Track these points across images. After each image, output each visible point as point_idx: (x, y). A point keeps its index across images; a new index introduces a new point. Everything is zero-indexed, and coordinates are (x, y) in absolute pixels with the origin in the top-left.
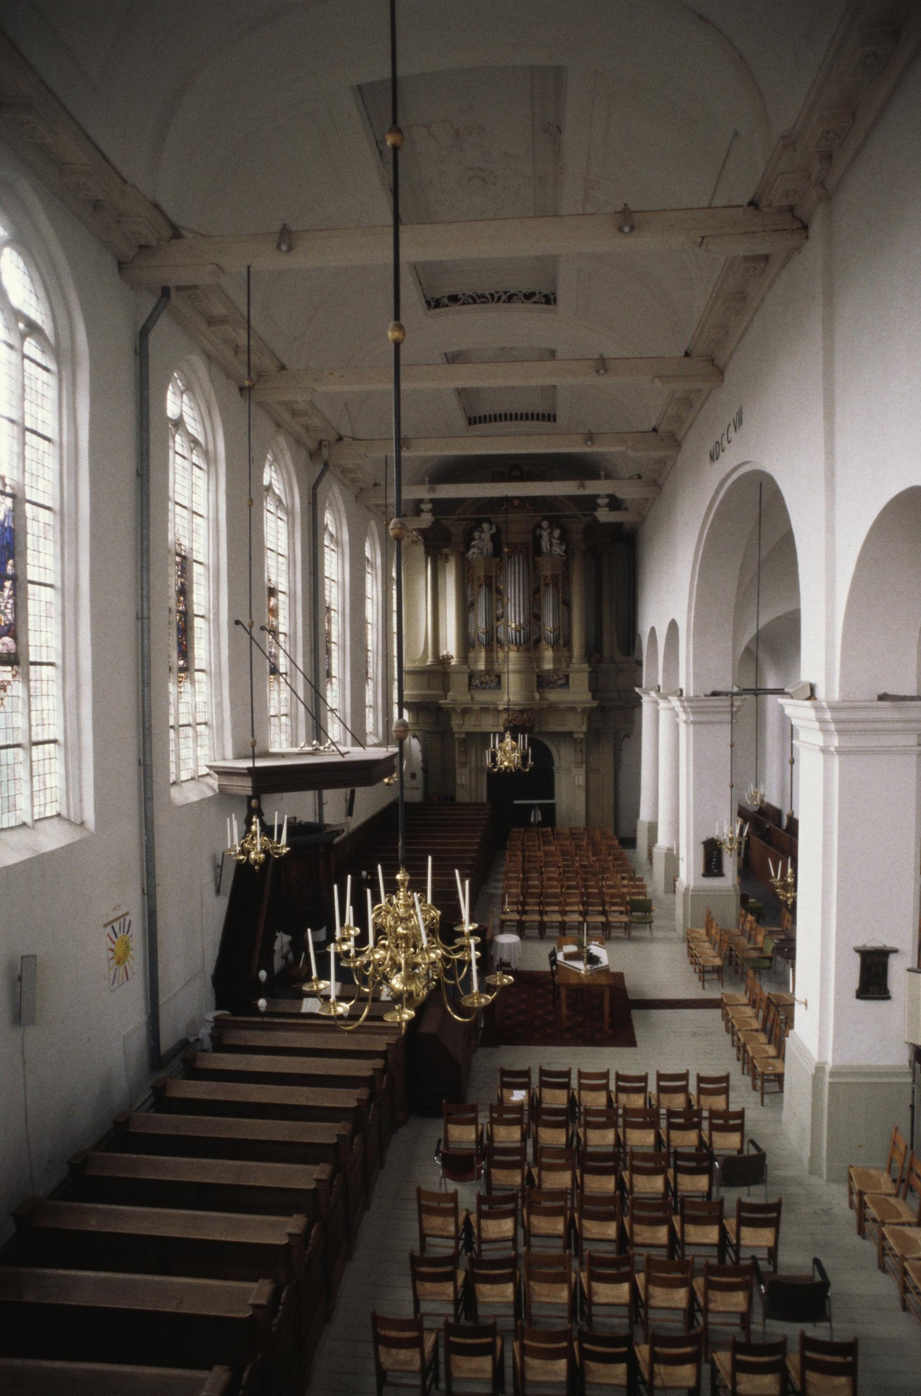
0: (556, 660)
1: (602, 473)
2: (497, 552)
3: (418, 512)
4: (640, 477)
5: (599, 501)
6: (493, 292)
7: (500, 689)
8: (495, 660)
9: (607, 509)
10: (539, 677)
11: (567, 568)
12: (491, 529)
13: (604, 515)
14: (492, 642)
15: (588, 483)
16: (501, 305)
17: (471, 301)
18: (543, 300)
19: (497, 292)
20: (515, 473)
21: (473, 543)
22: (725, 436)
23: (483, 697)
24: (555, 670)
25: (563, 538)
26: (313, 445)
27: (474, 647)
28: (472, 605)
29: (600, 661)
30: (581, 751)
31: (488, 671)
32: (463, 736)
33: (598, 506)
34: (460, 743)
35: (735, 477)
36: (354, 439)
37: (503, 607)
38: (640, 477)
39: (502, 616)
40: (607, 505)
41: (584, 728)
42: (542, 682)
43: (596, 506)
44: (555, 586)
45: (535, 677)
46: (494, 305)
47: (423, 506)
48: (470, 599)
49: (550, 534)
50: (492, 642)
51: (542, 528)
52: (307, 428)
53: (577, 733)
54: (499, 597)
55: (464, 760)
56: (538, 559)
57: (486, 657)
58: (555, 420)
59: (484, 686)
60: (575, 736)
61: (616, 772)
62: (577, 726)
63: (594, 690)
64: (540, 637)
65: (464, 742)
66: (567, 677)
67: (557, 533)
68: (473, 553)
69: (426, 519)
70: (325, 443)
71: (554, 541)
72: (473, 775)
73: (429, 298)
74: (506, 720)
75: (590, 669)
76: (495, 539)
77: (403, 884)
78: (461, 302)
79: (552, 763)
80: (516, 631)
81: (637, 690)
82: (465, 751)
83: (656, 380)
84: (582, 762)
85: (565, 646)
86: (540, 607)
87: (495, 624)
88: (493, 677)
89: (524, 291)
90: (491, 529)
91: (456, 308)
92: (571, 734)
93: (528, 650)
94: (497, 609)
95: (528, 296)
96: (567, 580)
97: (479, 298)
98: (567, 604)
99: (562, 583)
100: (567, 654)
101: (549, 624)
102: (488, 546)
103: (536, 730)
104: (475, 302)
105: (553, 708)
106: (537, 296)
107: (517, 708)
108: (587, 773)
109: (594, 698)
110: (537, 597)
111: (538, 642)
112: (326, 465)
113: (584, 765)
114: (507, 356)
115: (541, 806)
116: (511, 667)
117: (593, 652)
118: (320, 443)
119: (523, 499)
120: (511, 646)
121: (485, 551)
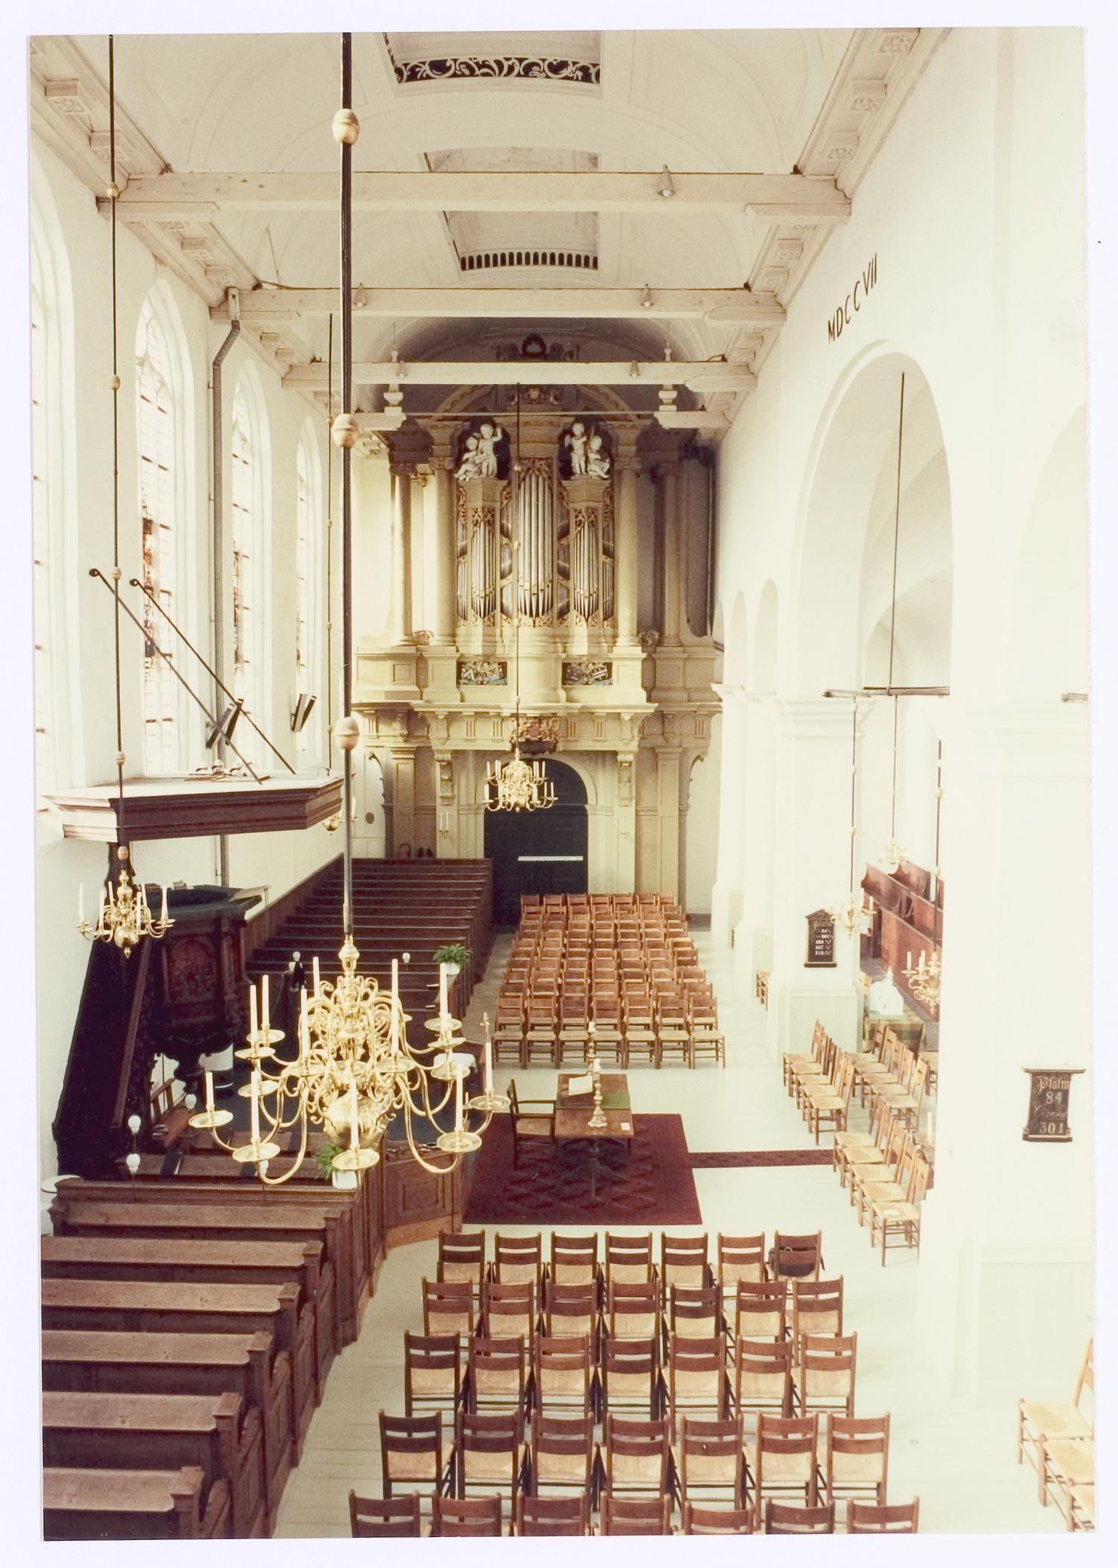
0: (594, 640)
1: (668, 352)
2: (503, 470)
3: (381, 405)
4: (724, 359)
5: (662, 395)
6: (501, 58)
8: (498, 639)
9: (674, 407)
11: (611, 498)
12: (494, 435)
13: (669, 418)
14: (491, 608)
15: (644, 366)
16: (513, 79)
17: (467, 72)
18: (580, 74)
19: (508, 59)
20: (534, 348)
21: (466, 456)
22: (851, 299)
23: (479, 696)
24: (591, 656)
25: (606, 451)
26: (215, 295)
27: (465, 618)
29: (659, 643)
32: (448, 757)
33: (661, 402)
34: (442, 767)
35: (863, 364)
36: (281, 287)
37: (511, 557)
38: (724, 359)
39: (510, 572)
40: (674, 402)
41: (634, 746)
42: (570, 674)
43: (657, 403)
44: (593, 524)
46: (502, 79)
47: (387, 396)
48: (460, 544)
49: (585, 444)
50: (491, 608)
51: (572, 435)
52: (207, 268)
53: (626, 753)
54: (505, 540)
56: (564, 483)
58: (595, 265)
59: (480, 679)
60: (620, 758)
61: (682, 813)
63: (651, 689)
65: (448, 766)
66: (609, 666)
67: (596, 443)
69: (394, 418)
70: (232, 292)
71: (592, 456)
73: (400, 65)
75: (644, 655)
76: (501, 449)
77: (349, 965)
78: (451, 72)
79: (584, 799)
81: (715, 687)
82: (450, 780)
83: (749, 209)
84: (630, 799)
85: (605, 619)
86: (567, 559)
87: (499, 583)
88: (496, 666)
89: (550, 59)
91: (441, 81)
92: (615, 754)
95: (556, 68)
96: (611, 515)
97: (480, 67)
98: (609, 553)
99: (604, 521)
100: (609, 631)
101: (582, 586)
102: (491, 461)
103: (560, 747)
104: (472, 74)
105: (588, 714)
106: (571, 68)
109: (649, 700)
111: (563, 612)
112: (235, 325)
114: (523, 164)
117: (651, 629)
118: (226, 293)
119: (544, 389)
120: (522, 616)
121: (484, 470)
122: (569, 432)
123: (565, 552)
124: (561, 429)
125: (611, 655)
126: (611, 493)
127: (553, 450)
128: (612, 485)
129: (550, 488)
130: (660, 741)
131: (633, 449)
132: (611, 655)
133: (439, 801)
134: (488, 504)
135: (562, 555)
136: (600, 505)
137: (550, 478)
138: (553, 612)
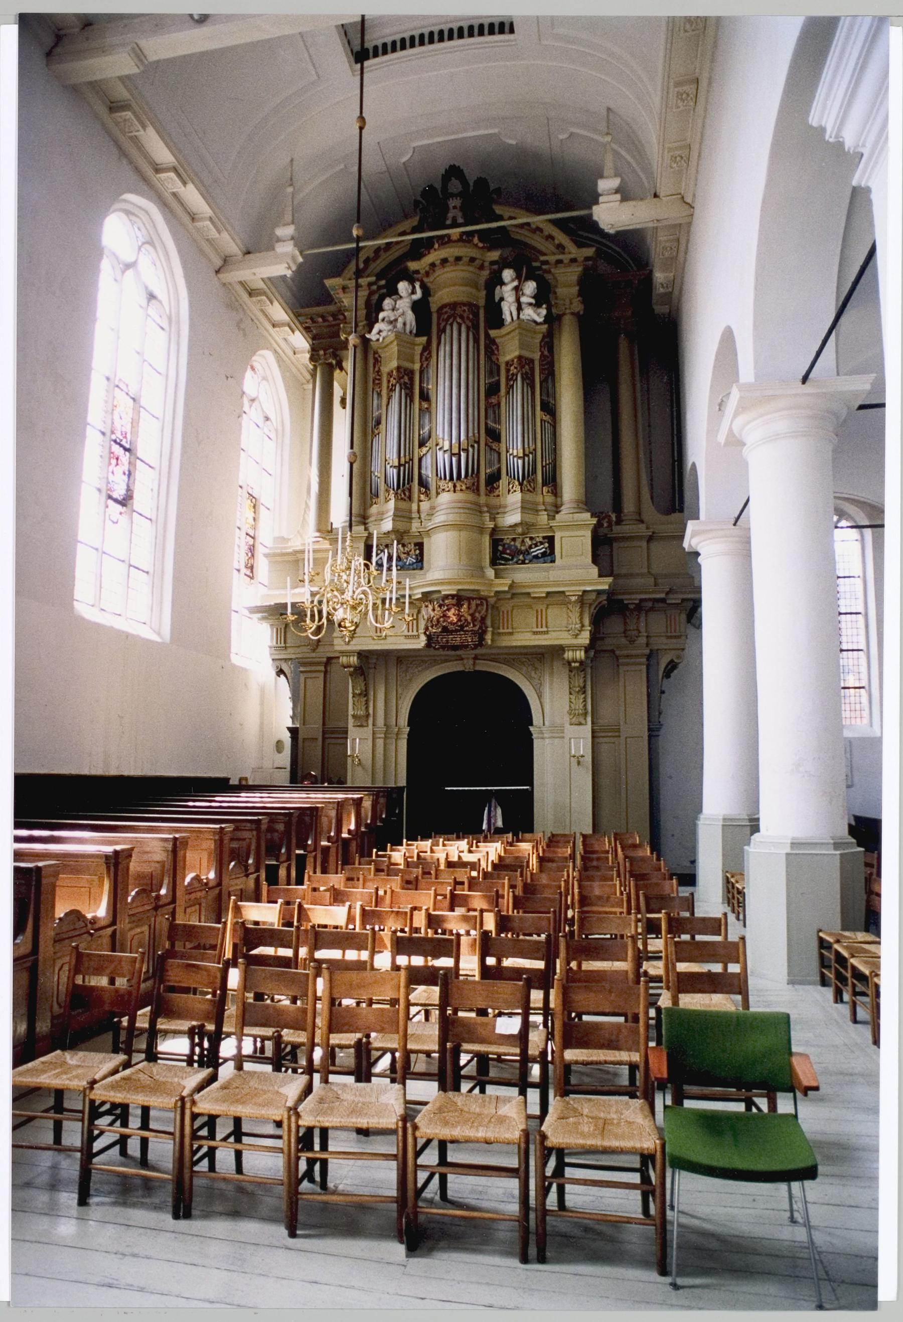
7: (422, 568)
9: (618, 197)
10: (495, 543)
11: (551, 350)
12: (413, 292)
24: (526, 526)
28: (378, 423)
30: (583, 690)
31: (400, 535)
41: (585, 638)
42: (503, 551)
45: (486, 541)
49: (517, 289)
50: (410, 484)
51: (502, 283)
53: (574, 648)
55: (361, 713)
56: (493, 333)
58: (512, 31)
61: (654, 731)
62: (569, 632)
64: (499, 469)
66: (551, 540)
67: (530, 287)
68: (380, 332)
71: (524, 299)
72: (380, 743)
74: (430, 620)
75: (594, 521)
80: (452, 455)
85: (544, 484)
86: (498, 420)
90: (413, 292)
93: (474, 488)
94: (421, 427)
98: (550, 409)
99: (540, 374)
100: (549, 499)
101: (514, 444)
107: (447, 590)
108: (593, 732)
110: (494, 400)
111: (493, 479)
113: (589, 719)
115: (503, 799)
116: (440, 518)
120: (442, 484)
121: (399, 325)
122: (496, 281)
123: (493, 410)
124: (486, 273)
125: (552, 523)
126: (549, 343)
129: (476, 341)
130: (623, 641)
131: (576, 289)
132: (552, 523)
133: (351, 721)
134: (407, 365)
136: (537, 356)
137: (476, 327)
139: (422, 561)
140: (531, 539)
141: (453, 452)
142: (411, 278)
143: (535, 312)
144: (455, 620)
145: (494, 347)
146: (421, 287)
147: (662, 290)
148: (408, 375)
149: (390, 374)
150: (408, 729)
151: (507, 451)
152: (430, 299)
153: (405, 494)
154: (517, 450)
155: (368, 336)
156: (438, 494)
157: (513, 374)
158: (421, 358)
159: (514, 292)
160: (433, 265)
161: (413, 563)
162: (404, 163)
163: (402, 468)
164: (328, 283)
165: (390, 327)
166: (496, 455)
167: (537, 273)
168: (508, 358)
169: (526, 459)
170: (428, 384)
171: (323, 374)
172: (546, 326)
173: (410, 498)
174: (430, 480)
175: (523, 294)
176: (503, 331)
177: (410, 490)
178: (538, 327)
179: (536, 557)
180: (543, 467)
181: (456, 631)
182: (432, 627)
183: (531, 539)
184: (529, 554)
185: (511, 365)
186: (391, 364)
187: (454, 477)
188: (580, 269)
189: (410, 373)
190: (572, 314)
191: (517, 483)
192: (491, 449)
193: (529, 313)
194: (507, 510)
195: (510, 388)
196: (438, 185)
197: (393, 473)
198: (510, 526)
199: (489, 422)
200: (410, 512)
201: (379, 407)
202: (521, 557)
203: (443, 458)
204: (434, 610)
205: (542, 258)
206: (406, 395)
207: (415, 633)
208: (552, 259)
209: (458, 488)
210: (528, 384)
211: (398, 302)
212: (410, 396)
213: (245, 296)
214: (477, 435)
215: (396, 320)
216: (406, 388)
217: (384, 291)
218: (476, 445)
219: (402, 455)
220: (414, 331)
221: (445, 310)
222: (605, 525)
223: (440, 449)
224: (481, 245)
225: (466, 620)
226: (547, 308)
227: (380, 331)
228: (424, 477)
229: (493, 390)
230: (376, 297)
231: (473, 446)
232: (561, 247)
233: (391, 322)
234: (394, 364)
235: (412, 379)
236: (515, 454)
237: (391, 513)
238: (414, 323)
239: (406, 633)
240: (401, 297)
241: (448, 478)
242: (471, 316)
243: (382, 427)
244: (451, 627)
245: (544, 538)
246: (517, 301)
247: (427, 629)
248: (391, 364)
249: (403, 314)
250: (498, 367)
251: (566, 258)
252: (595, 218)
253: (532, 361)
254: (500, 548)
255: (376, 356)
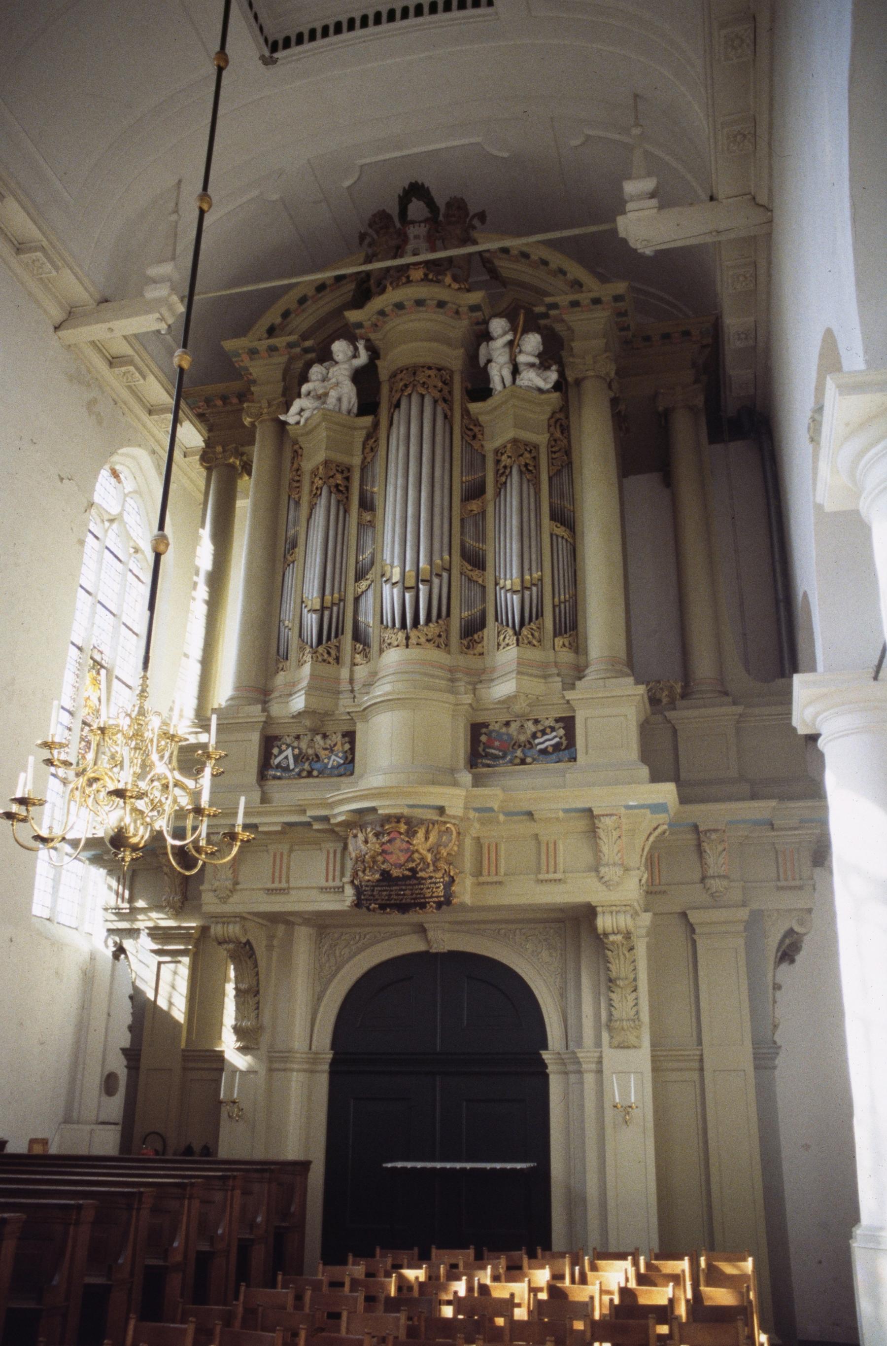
2: (367, 405)
7: (352, 774)
8: (345, 686)
9: (654, 202)
10: (476, 730)
11: (565, 429)
23: (296, 797)
28: (294, 545)
37: (374, 541)
44: (530, 472)
54: (368, 517)
57: (313, 676)
66: (568, 723)
67: (532, 342)
76: (365, 379)
86: (481, 536)
88: (338, 738)
93: (441, 642)
94: (359, 550)
98: (565, 518)
100: (566, 656)
110: (474, 506)
111: (473, 629)
120: (387, 634)
121: (331, 400)
123: (476, 523)
126: (562, 423)
127: (454, 359)
128: (565, 408)
129: (448, 418)
135: (470, 528)
136: (541, 439)
138: (456, 625)
139: (352, 761)
140: (536, 722)
141: (407, 584)
142: (349, 334)
143: (538, 375)
144: (403, 860)
145: (476, 429)
146: (367, 348)
147: (739, 344)
148: (342, 472)
149: (314, 473)
150: (329, 1056)
151: (496, 584)
152: (378, 362)
153: (329, 653)
154: (511, 578)
155: (282, 418)
156: (381, 651)
157: (505, 467)
158: (364, 448)
159: (507, 350)
160: (382, 313)
161: (339, 765)
162: (348, 188)
163: (327, 613)
164: (229, 345)
165: (317, 404)
166: (478, 590)
167: (542, 322)
168: (498, 443)
169: (527, 593)
170: (373, 486)
171: (219, 481)
172: (557, 395)
173: (337, 659)
174: (371, 630)
175: (520, 352)
176: (491, 402)
177: (338, 648)
178: (543, 396)
179: (544, 752)
180: (554, 607)
181: (405, 878)
182: (364, 871)
183: (536, 722)
184: (532, 747)
185: (502, 454)
186: (315, 456)
187: (409, 623)
188: (606, 314)
189: (345, 471)
190: (598, 377)
191: (510, 631)
192: (470, 580)
193: (531, 378)
194: (496, 675)
195: (501, 487)
196: (394, 212)
197: (311, 620)
198: (499, 702)
199: (468, 540)
200: (337, 680)
201: (296, 523)
202: (519, 753)
203: (391, 595)
204: (366, 842)
205: (548, 300)
206: (339, 502)
207: (338, 883)
208: (563, 300)
209: (413, 641)
210: (529, 481)
211: (331, 371)
212: (344, 505)
213: (101, 365)
214: (446, 557)
215: (326, 394)
216: (339, 491)
217: (312, 355)
218: (445, 575)
219: (328, 591)
220: (355, 410)
221: (399, 376)
222: (665, 701)
223: (386, 581)
224: (456, 286)
225: (423, 859)
226: (558, 371)
227: (302, 410)
228: (362, 626)
229: (475, 491)
230: (300, 364)
231: (439, 576)
232: (577, 285)
233: (319, 397)
234: (321, 456)
235: (347, 479)
236: (508, 587)
237: (304, 683)
238: (354, 400)
239: (323, 883)
240: (337, 363)
241: (397, 625)
242: (440, 384)
243: (300, 550)
244: (396, 872)
245: (557, 720)
246: (516, 365)
247: (355, 875)
248: (315, 456)
249: (337, 384)
250: (484, 457)
251: (584, 297)
252: (622, 234)
253: (536, 447)
254: (484, 738)
255: (296, 447)
